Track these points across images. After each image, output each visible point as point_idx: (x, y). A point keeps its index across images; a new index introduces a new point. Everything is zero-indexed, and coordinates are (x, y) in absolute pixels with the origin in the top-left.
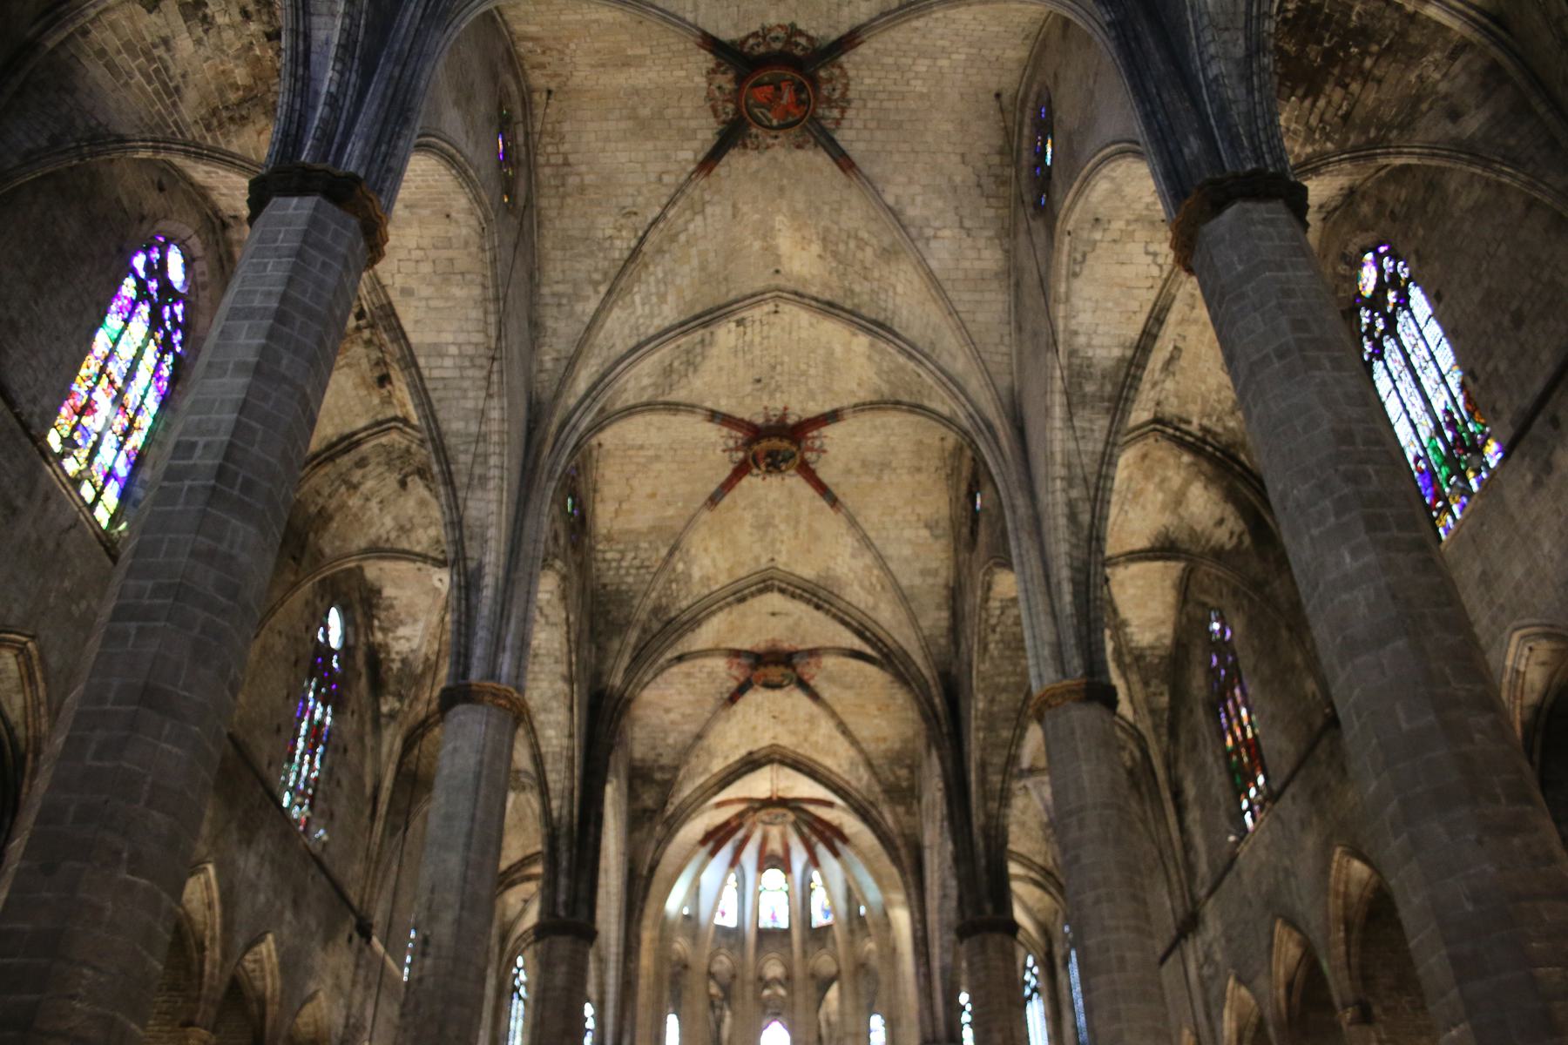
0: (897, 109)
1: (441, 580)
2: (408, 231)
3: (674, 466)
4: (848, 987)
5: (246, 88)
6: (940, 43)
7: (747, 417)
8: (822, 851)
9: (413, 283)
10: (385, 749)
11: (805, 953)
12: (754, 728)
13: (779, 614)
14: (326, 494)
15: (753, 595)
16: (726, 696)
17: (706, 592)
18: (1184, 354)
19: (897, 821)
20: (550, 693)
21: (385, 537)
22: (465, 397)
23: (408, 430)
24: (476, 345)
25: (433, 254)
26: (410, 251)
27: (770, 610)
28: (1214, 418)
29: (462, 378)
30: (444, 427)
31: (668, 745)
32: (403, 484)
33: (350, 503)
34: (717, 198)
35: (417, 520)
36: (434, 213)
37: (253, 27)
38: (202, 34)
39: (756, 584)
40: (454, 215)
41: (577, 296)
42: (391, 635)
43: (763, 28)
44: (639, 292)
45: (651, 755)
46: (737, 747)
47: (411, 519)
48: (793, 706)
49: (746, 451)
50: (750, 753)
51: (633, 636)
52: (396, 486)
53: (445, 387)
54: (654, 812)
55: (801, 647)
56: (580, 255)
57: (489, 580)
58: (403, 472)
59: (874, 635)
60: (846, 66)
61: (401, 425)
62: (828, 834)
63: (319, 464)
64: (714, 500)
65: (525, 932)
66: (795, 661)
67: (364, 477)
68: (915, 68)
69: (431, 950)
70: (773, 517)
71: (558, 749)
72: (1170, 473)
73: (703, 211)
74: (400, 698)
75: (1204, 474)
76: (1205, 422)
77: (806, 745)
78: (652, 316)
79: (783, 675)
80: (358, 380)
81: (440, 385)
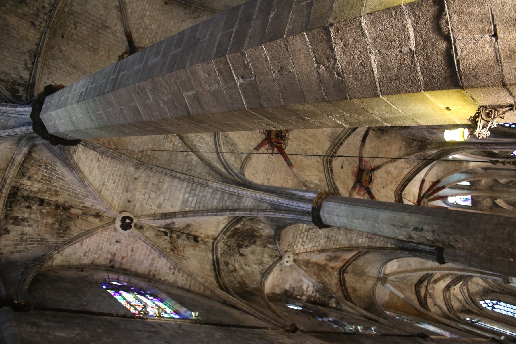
0: (160, 37)
1: (287, 262)
2: (137, 196)
3: (273, 175)
4: (498, 195)
5: (55, 221)
6: (140, 9)
7: (261, 140)
8: (441, 193)
9: (157, 202)
10: (351, 310)
11: (481, 210)
12: (386, 196)
13: (342, 165)
14: (233, 279)
15: (331, 167)
17: (325, 182)
19: (433, 149)
20: (344, 236)
21: (260, 270)
22: (206, 197)
23: (219, 238)
24: (187, 186)
25: (148, 191)
26: (144, 199)
27: (340, 168)
29: (198, 196)
30: (214, 207)
32: (242, 255)
33: (241, 274)
35: (259, 258)
36: (133, 183)
37: (35, 207)
38: (27, 223)
39: (327, 165)
40: (136, 176)
41: (189, 163)
42: (305, 293)
47: (257, 259)
48: (380, 178)
49: (275, 148)
52: (241, 258)
53: (200, 203)
55: (358, 164)
56: (176, 158)
57: (275, 199)
58: (237, 252)
60: (139, 45)
61: (216, 241)
62: (435, 188)
63: (220, 276)
64: (290, 165)
65: (448, 309)
66: (363, 167)
67: (233, 266)
68: (147, 24)
69: (420, 227)
70: (303, 149)
71: (367, 240)
74: (332, 297)
77: (397, 179)
78: (208, 144)
79: (367, 174)
80: (192, 248)
81: (198, 205)
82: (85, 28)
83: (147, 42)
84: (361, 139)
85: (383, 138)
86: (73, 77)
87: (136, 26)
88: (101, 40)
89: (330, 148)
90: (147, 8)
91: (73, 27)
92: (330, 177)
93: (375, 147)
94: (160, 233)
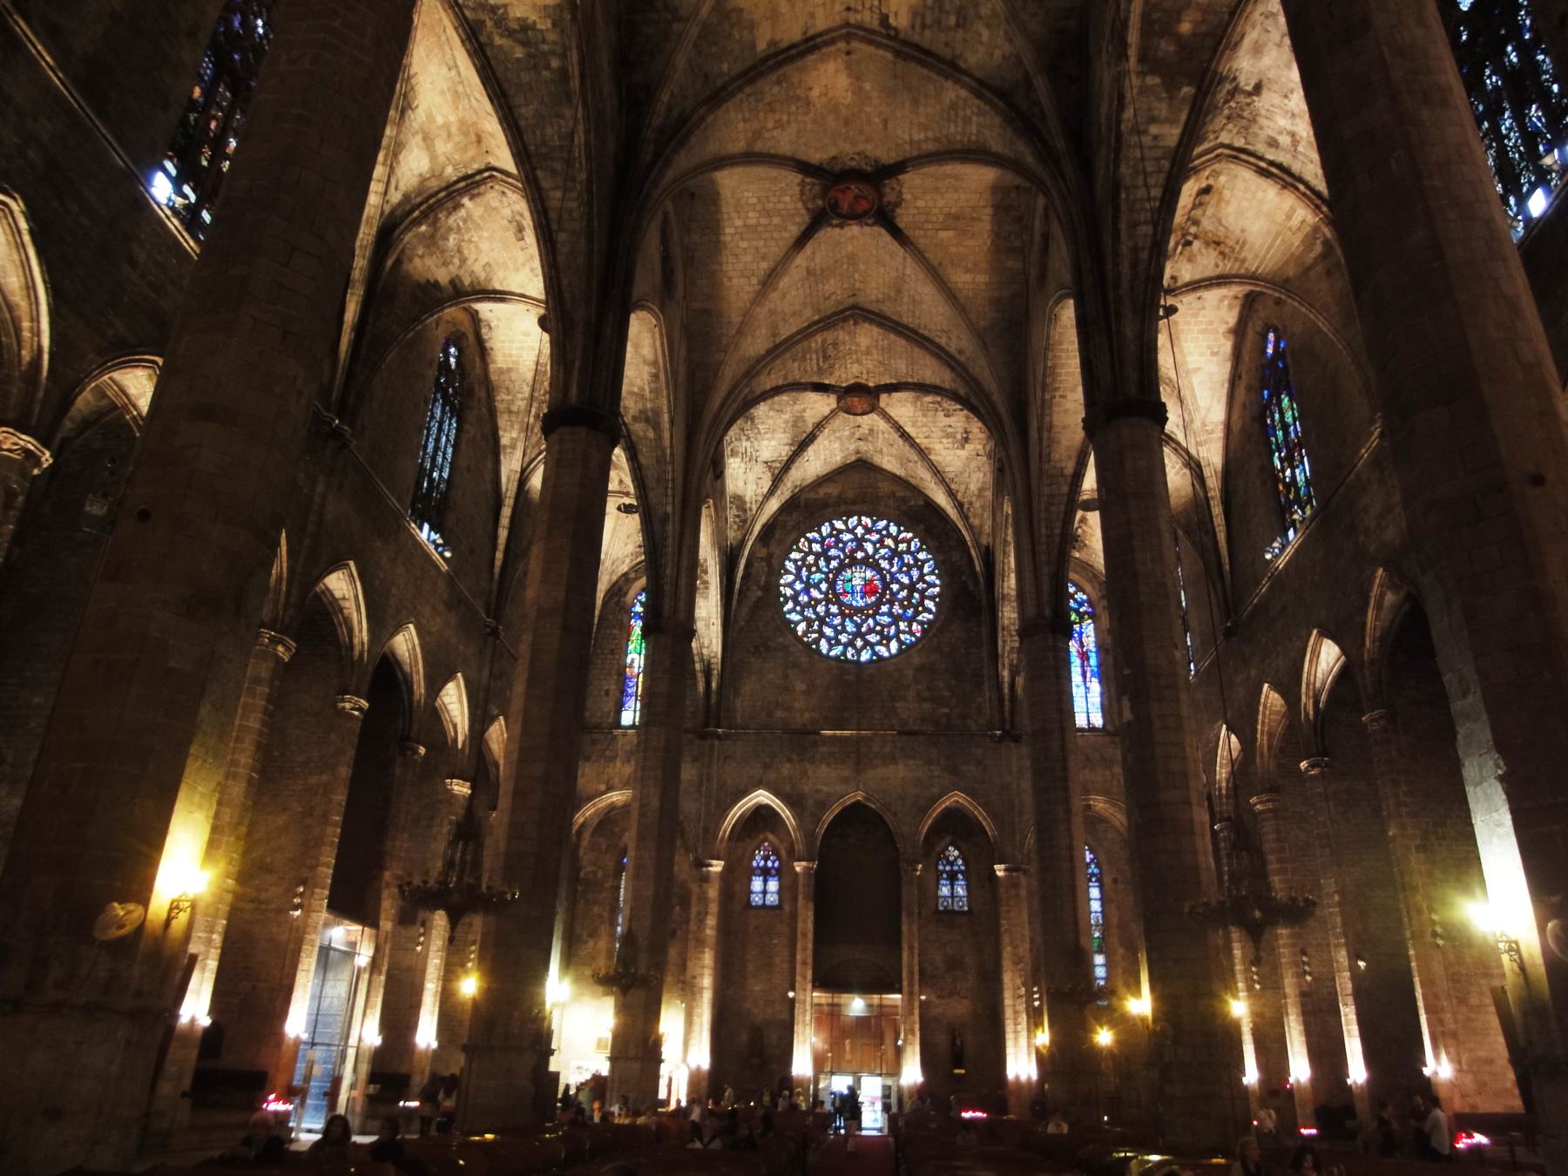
6: (744, 244)
18: (514, 240)
28: (461, 224)
32: (1258, 89)
34: (900, 141)
43: (862, 226)
44: (971, 133)
52: (1265, 93)
58: (1249, 100)
60: (804, 212)
68: (757, 215)
72: (450, 146)
73: (911, 141)
75: (429, 178)
76: (463, 212)
80: (1223, 205)
82: (827, 287)
83: (787, 199)
86: (917, 298)
87: (776, 235)
88: (831, 261)
90: (732, 230)
91: (833, 297)
94: (1186, 253)
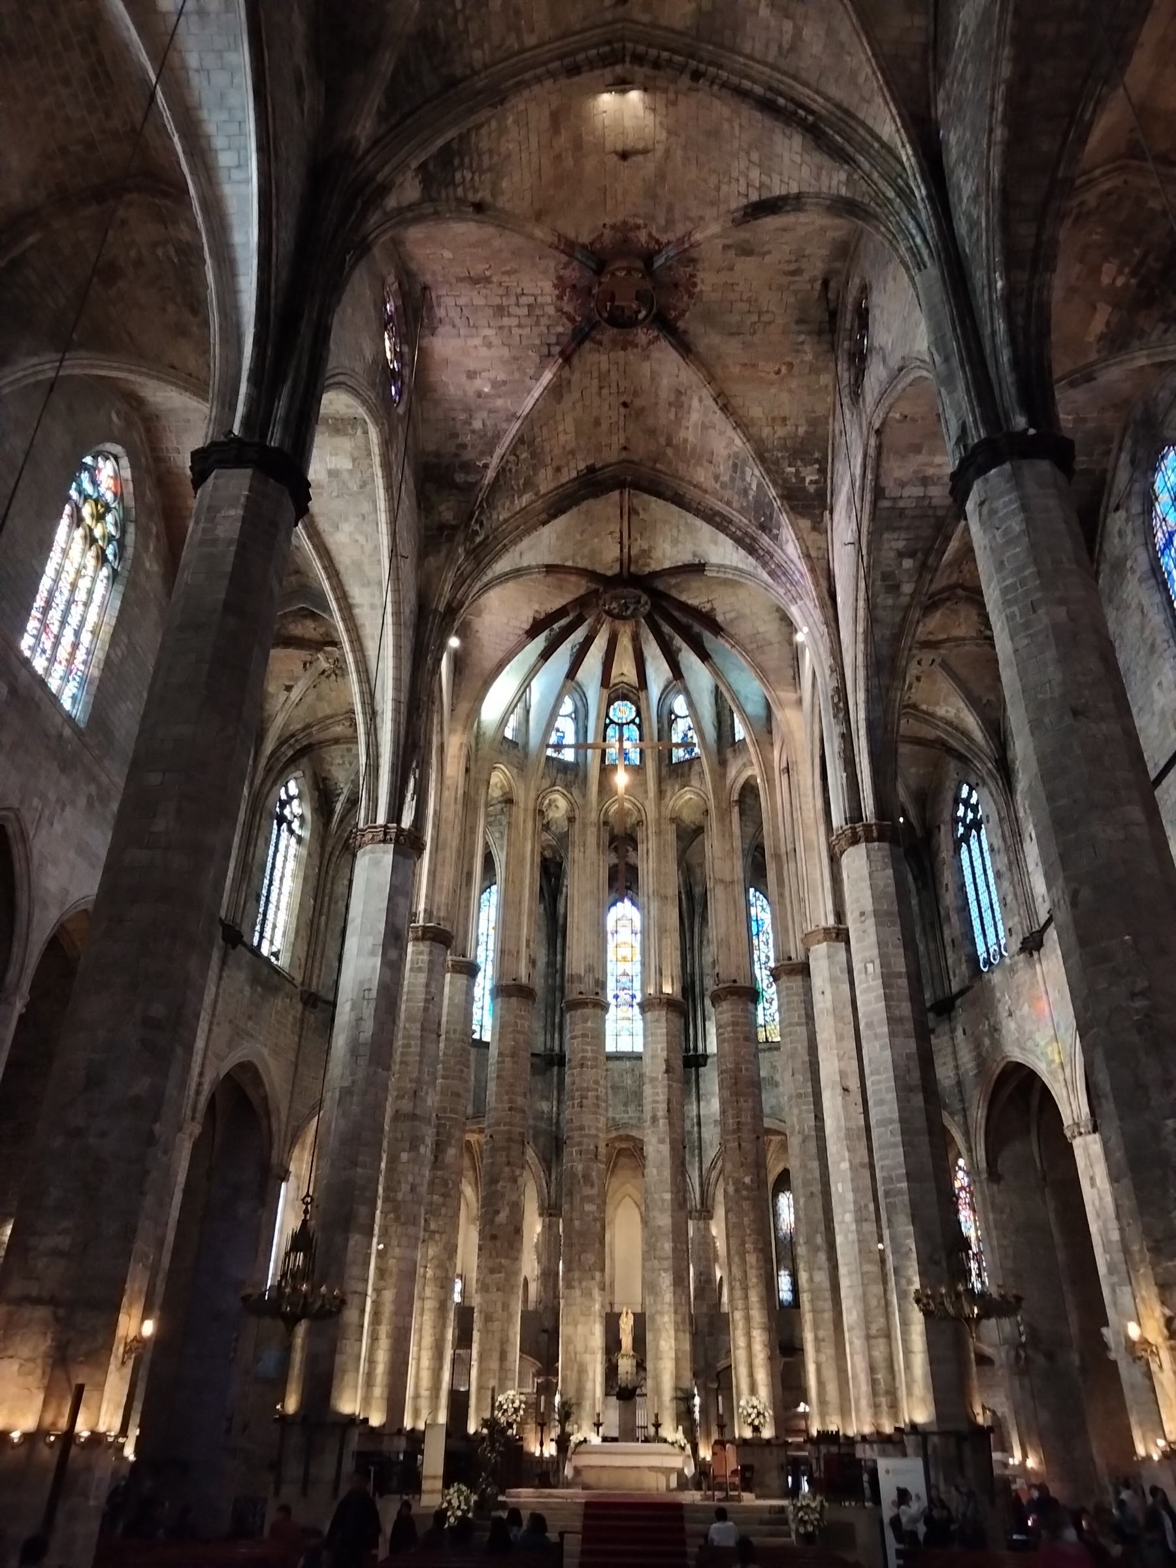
11: (661, 794)
12: (597, 423)
13: (637, 152)
15: (592, 65)
16: (556, 350)
17: (512, 42)
27: (619, 148)
31: (473, 432)
45: (451, 447)
46: (572, 452)
50: (591, 469)
51: (387, 62)
54: (455, 528)
59: (792, 100)
62: (697, 628)
65: (293, 736)
79: (638, 297)
84: (754, 197)
85: (802, 338)
89: (673, 31)
92: (545, 63)
93: (760, 314)
